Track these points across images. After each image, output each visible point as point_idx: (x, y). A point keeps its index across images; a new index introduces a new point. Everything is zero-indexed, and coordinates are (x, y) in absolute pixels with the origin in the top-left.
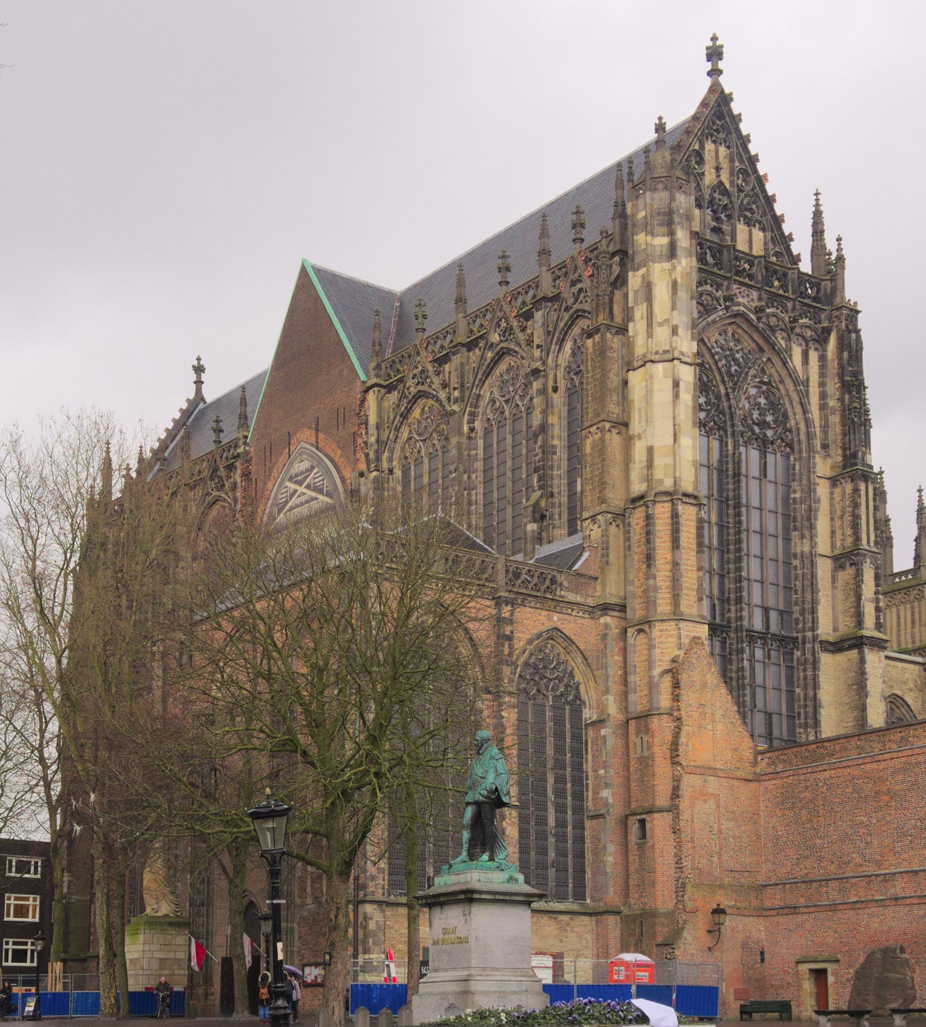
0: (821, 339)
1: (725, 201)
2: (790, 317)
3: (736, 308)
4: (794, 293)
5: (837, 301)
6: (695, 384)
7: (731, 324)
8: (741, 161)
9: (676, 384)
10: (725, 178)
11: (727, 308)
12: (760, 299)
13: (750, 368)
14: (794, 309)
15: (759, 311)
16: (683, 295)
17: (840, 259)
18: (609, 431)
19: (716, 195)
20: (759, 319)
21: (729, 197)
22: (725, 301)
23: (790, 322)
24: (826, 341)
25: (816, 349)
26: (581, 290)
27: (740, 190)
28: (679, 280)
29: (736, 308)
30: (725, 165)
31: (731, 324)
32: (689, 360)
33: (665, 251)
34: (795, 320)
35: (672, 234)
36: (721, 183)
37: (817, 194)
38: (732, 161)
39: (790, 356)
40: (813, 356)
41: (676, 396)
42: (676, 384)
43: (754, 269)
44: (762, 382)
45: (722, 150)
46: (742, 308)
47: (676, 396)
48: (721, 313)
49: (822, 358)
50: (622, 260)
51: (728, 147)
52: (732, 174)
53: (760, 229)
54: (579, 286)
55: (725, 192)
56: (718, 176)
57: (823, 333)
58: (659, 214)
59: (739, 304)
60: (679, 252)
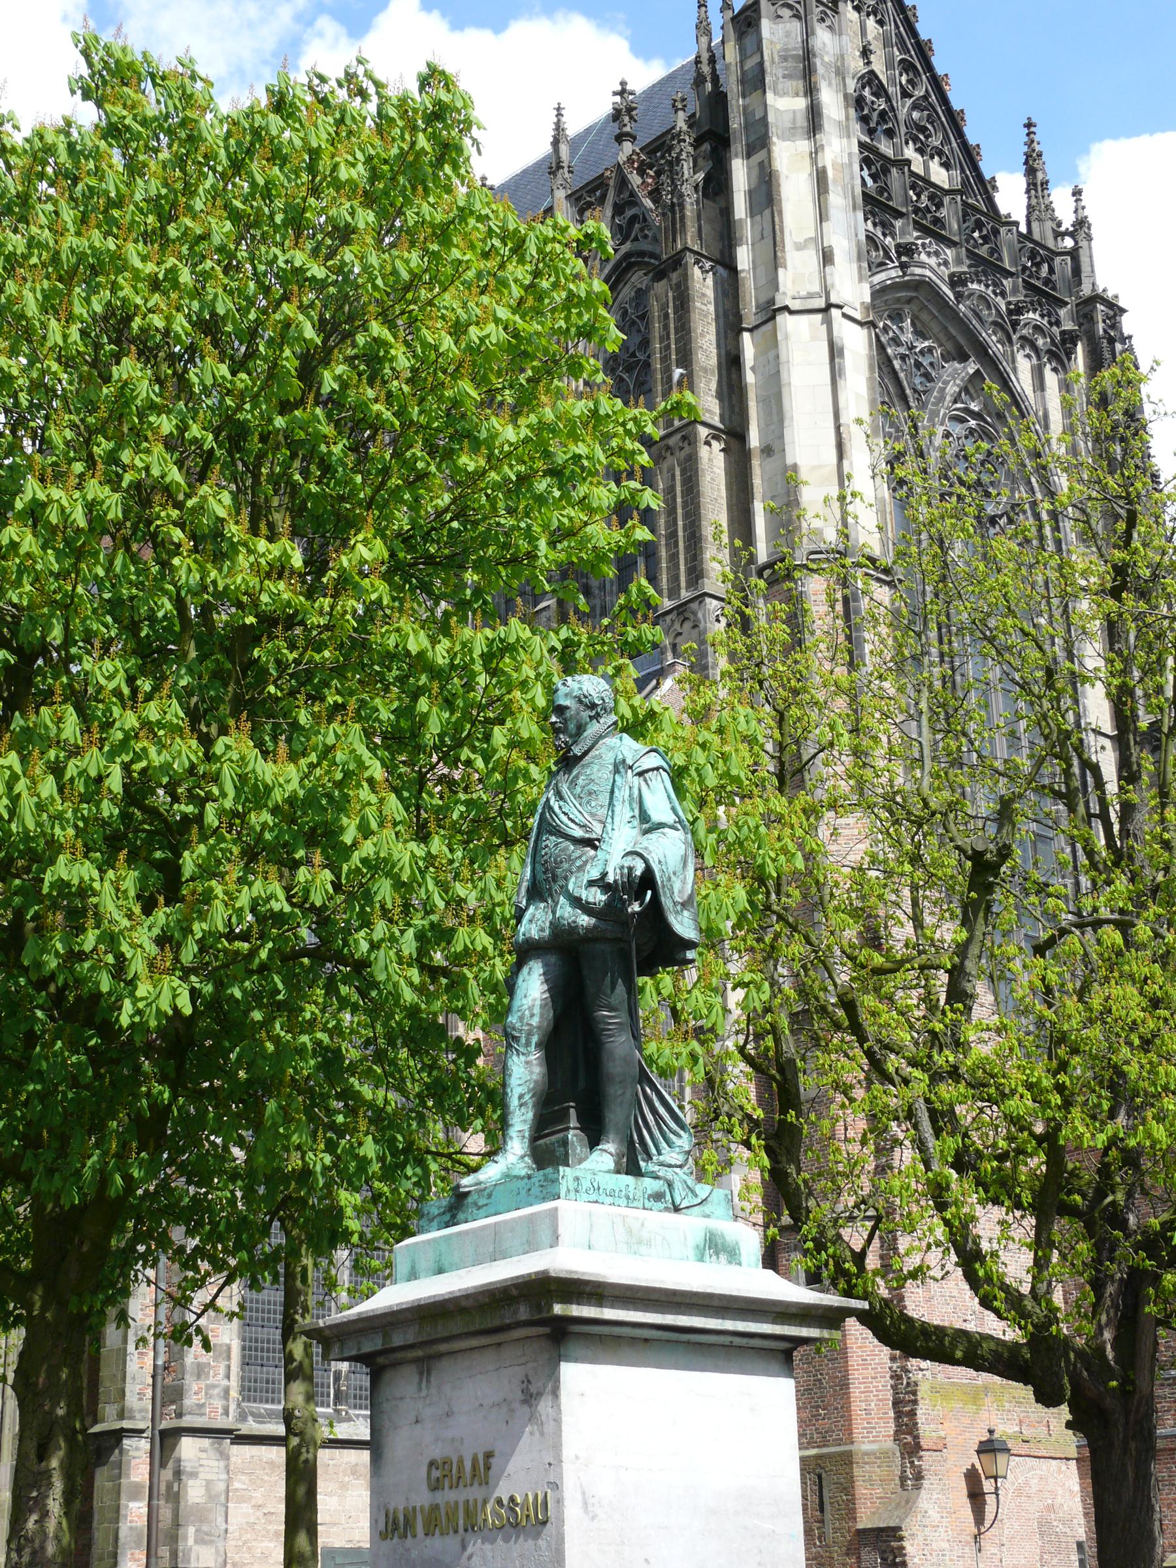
0: (1060, 355)
1: (882, 105)
2: (1009, 303)
3: (918, 271)
4: (1014, 262)
5: (1086, 290)
6: (871, 358)
7: (909, 301)
8: (904, 49)
9: (835, 352)
10: (878, 66)
11: (903, 266)
12: (959, 261)
13: (946, 383)
14: (1015, 290)
15: (956, 281)
16: (837, 200)
17: (1081, 224)
18: (708, 443)
19: (867, 92)
20: (959, 296)
21: (888, 100)
22: (899, 254)
23: (1010, 312)
24: (1069, 353)
25: (1055, 370)
26: (633, 219)
27: (905, 94)
28: (830, 174)
29: (918, 271)
30: (877, 47)
31: (909, 301)
32: (858, 315)
33: (802, 122)
34: (1019, 310)
35: (811, 91)
36: (872, 72)
37: (1029, 125)
38: (887, 44)
39: (1015, 370)
40: (1051, 379)
41: (836, 374)
42: (835, 352)
43: (943, 213)
44: (967, 411)
45: (871, 22)
46: (928, 273)
47: (836, 374)
48: (893, 273)
49: (1066, 386)
50: (714, 150)
51: (881, 23)
52: (889, 65)
53: (942, 165)
54: (629, 213)
55: (880, 91)
56: (869, 63)
57: (1063, 341)
58: (785, 59)
59: (922, 265)
60: (827, 125)
